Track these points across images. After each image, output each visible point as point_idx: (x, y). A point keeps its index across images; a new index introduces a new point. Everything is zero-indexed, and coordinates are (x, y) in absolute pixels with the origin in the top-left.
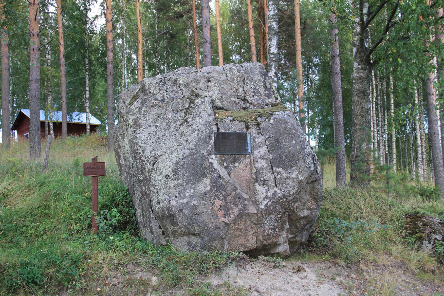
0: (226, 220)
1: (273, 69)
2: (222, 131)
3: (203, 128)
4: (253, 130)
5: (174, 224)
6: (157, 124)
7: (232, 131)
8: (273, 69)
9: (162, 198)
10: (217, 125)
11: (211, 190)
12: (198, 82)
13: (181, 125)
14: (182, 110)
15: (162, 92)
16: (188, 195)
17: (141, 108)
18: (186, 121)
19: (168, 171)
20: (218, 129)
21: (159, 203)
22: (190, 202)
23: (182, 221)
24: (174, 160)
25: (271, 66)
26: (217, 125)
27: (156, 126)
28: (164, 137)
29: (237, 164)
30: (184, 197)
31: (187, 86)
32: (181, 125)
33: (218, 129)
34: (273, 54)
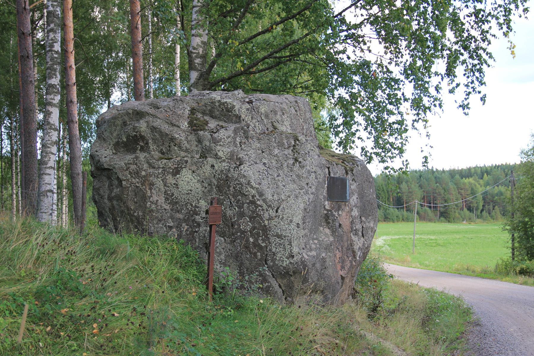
0: (342, 273)
1: (58, 74)
2: (332, 175)
3: (319, 171)
4: (349, 177)
5: (305, 280)
6: (264, 161)
7: (337, 176)
8: (58, 74)
9: (295, 250)
10: (329, 168)
11: (334, 240)
12: (276, 113)
13: (294, 164)
14: (289, 147)
15: (254, 121)
16: (313, 246)
17: (234, 139)
18: (296, 160)
19: (298, 219)
20: (329, 173)
21: (293, 257)
22: (320, 255)
23: (313, 276)
24: (302, 206)
25: (55, 70)
26: (329, 168)
27: (264, 164)
28: (279, 178)
29: (340, 213)
30: (311, 250)
31: (267, 116)
32: (294, 164)
33: (329, 173)
34: (57, 52)
